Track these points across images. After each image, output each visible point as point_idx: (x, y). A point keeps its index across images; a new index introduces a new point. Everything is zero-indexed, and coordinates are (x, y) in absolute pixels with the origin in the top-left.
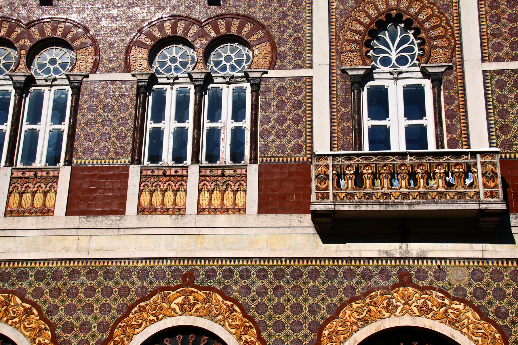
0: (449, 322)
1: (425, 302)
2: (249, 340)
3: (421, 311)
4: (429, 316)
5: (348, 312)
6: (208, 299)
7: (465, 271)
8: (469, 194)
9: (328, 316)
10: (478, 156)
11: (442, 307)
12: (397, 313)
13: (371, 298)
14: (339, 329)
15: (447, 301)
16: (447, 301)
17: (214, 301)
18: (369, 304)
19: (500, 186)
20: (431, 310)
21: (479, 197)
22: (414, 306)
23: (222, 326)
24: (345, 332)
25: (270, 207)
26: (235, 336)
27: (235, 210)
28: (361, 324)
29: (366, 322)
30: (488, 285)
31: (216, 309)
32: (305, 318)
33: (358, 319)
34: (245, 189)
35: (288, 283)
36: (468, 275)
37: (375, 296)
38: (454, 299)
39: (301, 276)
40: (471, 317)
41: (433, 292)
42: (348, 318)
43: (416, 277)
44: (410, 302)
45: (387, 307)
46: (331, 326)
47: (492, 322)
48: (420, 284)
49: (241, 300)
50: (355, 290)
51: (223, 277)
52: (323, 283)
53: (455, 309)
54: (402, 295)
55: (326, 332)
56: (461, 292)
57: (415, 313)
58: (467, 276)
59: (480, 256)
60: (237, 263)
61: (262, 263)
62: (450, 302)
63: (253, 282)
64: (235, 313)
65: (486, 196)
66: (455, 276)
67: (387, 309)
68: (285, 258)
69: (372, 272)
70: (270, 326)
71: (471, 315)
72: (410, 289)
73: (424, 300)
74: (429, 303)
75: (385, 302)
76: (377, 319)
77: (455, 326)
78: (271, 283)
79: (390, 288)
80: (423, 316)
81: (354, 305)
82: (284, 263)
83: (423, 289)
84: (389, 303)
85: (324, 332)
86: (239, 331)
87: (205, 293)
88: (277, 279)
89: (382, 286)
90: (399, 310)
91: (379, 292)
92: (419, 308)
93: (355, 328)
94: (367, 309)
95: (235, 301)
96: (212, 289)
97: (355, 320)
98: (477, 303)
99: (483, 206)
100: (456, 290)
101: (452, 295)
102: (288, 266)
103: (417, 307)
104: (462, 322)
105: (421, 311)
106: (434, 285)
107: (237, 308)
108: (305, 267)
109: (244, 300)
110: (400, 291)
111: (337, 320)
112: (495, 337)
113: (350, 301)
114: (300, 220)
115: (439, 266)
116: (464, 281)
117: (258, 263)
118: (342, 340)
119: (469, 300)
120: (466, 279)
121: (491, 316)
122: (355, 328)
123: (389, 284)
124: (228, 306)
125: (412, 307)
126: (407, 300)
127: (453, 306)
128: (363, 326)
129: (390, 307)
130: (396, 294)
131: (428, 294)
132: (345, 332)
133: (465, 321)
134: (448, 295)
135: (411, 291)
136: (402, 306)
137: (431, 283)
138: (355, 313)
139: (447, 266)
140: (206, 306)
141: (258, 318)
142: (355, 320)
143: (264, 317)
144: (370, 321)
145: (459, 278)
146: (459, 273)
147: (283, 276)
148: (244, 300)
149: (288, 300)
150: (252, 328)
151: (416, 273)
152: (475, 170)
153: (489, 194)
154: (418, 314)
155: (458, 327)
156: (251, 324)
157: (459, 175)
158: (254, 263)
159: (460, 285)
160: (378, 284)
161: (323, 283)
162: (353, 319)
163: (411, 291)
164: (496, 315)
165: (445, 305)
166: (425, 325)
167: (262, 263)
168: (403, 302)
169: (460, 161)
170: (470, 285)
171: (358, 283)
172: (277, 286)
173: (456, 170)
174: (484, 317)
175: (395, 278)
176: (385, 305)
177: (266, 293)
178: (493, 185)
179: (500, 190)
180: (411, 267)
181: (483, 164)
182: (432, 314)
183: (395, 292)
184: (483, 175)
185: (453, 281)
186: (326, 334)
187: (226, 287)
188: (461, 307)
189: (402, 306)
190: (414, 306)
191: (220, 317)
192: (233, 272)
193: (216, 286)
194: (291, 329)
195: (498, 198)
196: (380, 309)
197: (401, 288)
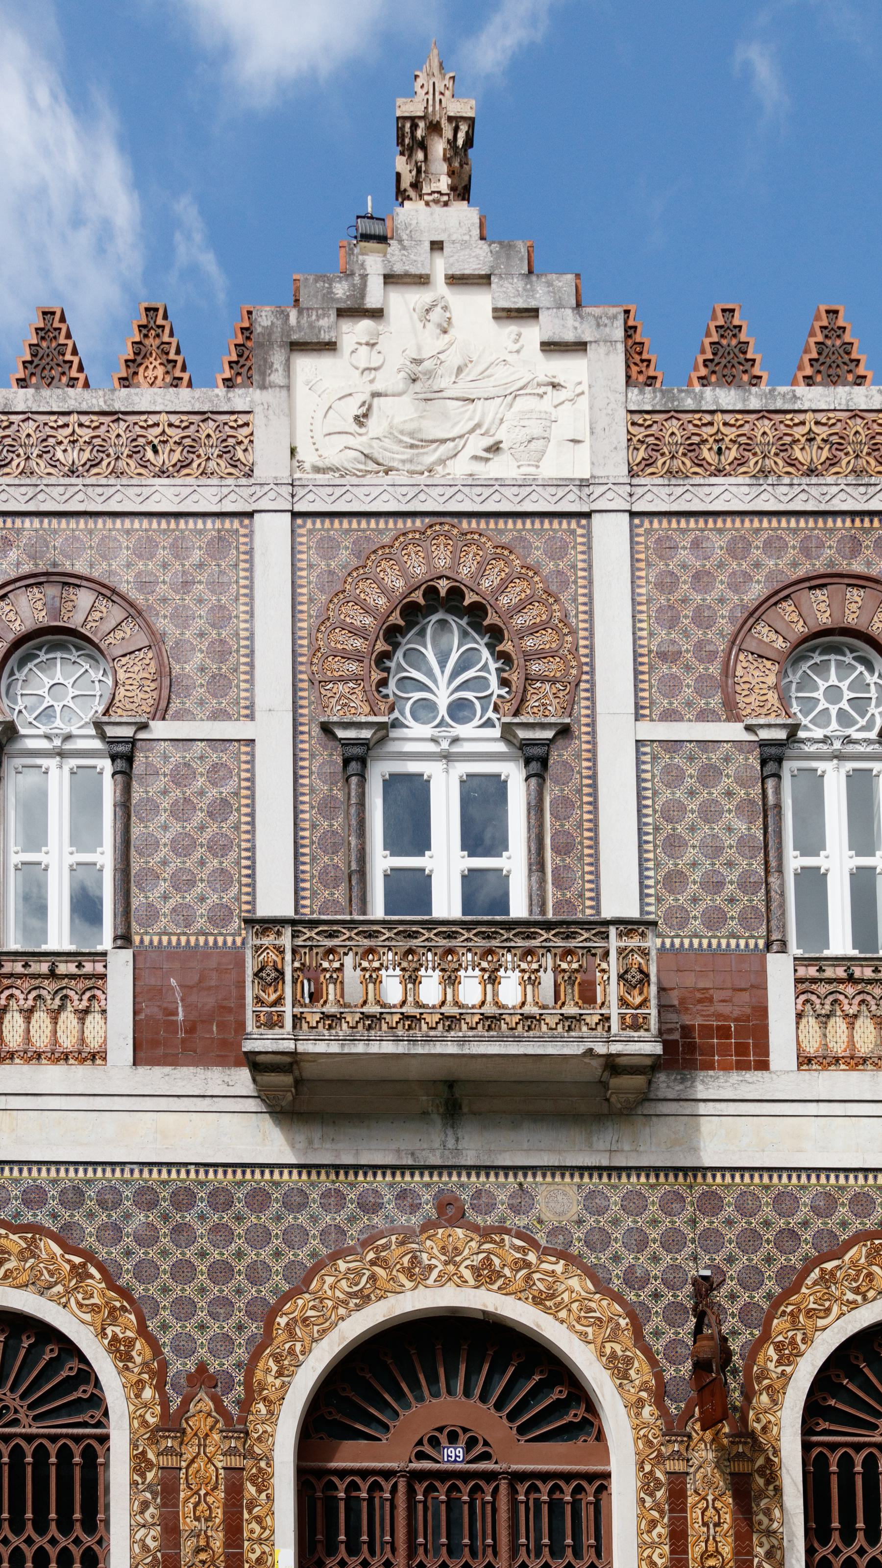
0: (534, 1297)
1: (488, 1258)
2: (121, 1336)
3: (478, 1276)
4: (495, 1287)
5: (329, 1280)
6: (31, 1251)
7: (571, 1193)
8: (588, 1021)
9: (286, 1287)
10: (613, 931)
11: (521, 1269)
12: (430, 1281)
13: (377, 1250)
14: (310, 1313)
15: (532, 1257)
16: (532, 1257)
17: (44, 1256)
18: (373, 1263)
19: (653, 1002)
20: (499, 1275)
21: (609, 1027)
22: (466, 1267)
23: (64, 1307)
24: (321, 1320)
25: (161, 1051)
26: (92, 1328)
27: (84, 1055)
28: (356, 1304)
29: (365, 1299)
30: (616, 1222)
31: (49, 1271)
32: (239, 1291)
33: (348, 1293)
34: (104, 1007)
35: (202, 1217)
36: (579, 1203)
37: (386, 1247)
38: (546, 1252)
39: (229, 1204)
40: (577, 1288)
41: (506, 1237)
42: (329, 1293)
43: (472, 1206)
44: (458, 1259)
45: (409, 1269)
46: (293, 1308)
47: (617, 1298)
48: (479, 1220)
49: (102, 1253)
50: (344, 1233)
51: (62, 1203)
52: (278, 1218)
53: (546, 1273)
54: (441, 1244)
55: (282, 1321)
56: (561, 1237)
57: (466, 1282)
58: (575, 1204)
59: (605, 1163)
60: (90, 1174)
61: (146, 1174)
62: (539, 1258)
63: (127, 1216)
64: (90, 1281)
65: (624, 1026)
66: (552, 1204)
67: (409, 1273)
68: (196, 1164)
69: (381, 1197)
70: (164, 1308)
71: (578, 1285)
72: (460, 1232)
73: (485, 1255)
74: (497, 1261)
75: (406, 1260)
76: (389, 1294)
77: (545, 1306)
78: (165, 1218)
79: (418, 1230)
80: (483, 1288)
81: (342, 1265)
82: (193, 1175)
83: (486, 1234)
84: (415, 1260)
85: (278, 1319)
86: (99, 1318)
87: (25, 1239)
88: (179, 1210)
89: (403, 1226)
90: (435, 1274)
91: (393, 1238)
92: (476, 1271)
93: (342, 1311)
94: (368, 1273)
95: (89, 1256)
96: (37, 1229)
97: (342, 1296)
98: (591, 1259)
99: (615, 1048)
100: (553, 1232)
101: (543, 1243)
102: (202, 1183)
103: (472, 1268)
104: (559, 1299)
105: (478, 1276)
106: (508, 1222)
107: (93, 1270)
108: (240, 1184)
109: (109, 1253)
110: (439, 1236)
111: (307, 1296)
112: (618, 1324)
113: (335, 1257)
114: (226, 1080)
115: (521, 1185)
116: (568, 1216)
117: (136, 1174)
118: (316, 1335)
119: (576, 1253)
120: (574, 1210)
121: (616, 1284)
122: (342, 1311)
123: (415, 1220)
124: (74, 1267)
125: (462, 1268)
126: (452, 1255)
127: (544, 1266)
128: (358, 1308)
129: (417, 1269)
130: (429, 1243)
131: (495, 1242)
132: (321, 1320)
133: (566, 1296)
134: (534, 1244)
135: (462, 1236)
136: (440, 1267)
137: (503, 1220)
138: (344, 1282)
139: (536, 1184)
140: (28, 1265)
141: (139, 1290)
142: (342, 1296)
143: (153, 1290)
144: (373, 1298)
145: (559, 1209)
146: (560, 1198)
147: (191, 1205)
148: (109, 1253)
149: (203, 1254)
150: (126, 1310)
151: (473, 1197)
152: (604, 965)
153: (629, 1021)
154: (472, 1282)
155: (550, 1308)
156: (125, 1304)
157: (570, 978)
158: (127, 1175)
159: (560, 1222)
160: (392, 1222)
161: (278, 1218)
162: (338, 1294)
163: (462, 1236)
164: (626, 1282)
165: (528, 1265)
166: (485, 1305)
167: (146, 1174)
168: (443, 1258)
169: (572, 944)
170: (580, 1222)
171: (352, 1219)
172: (179, 1225)
173: (564, 966)
174: (602, 1287)
175: (429, 1209)
176: (406, 1265)
177: (156, 1239)
178: (638, 1000)
179: (653, 1012)
180: (462, 1185)
181: (620, 951)
182: (500, 1282)
183: (428, 1238)
184: (621, 977)
185: (547, 1216)
186: (283, 1325)
187: (68, 1227)
188: (559, 1268)
189: (440, 1267)
190: (466, 1267)
191: (59, 1288)
192: (82, 1194)
193: (48, 1223)
194: (210, 1314)
195: (647, 1030)
196: (394, 1273)
197: (440, 1231)
